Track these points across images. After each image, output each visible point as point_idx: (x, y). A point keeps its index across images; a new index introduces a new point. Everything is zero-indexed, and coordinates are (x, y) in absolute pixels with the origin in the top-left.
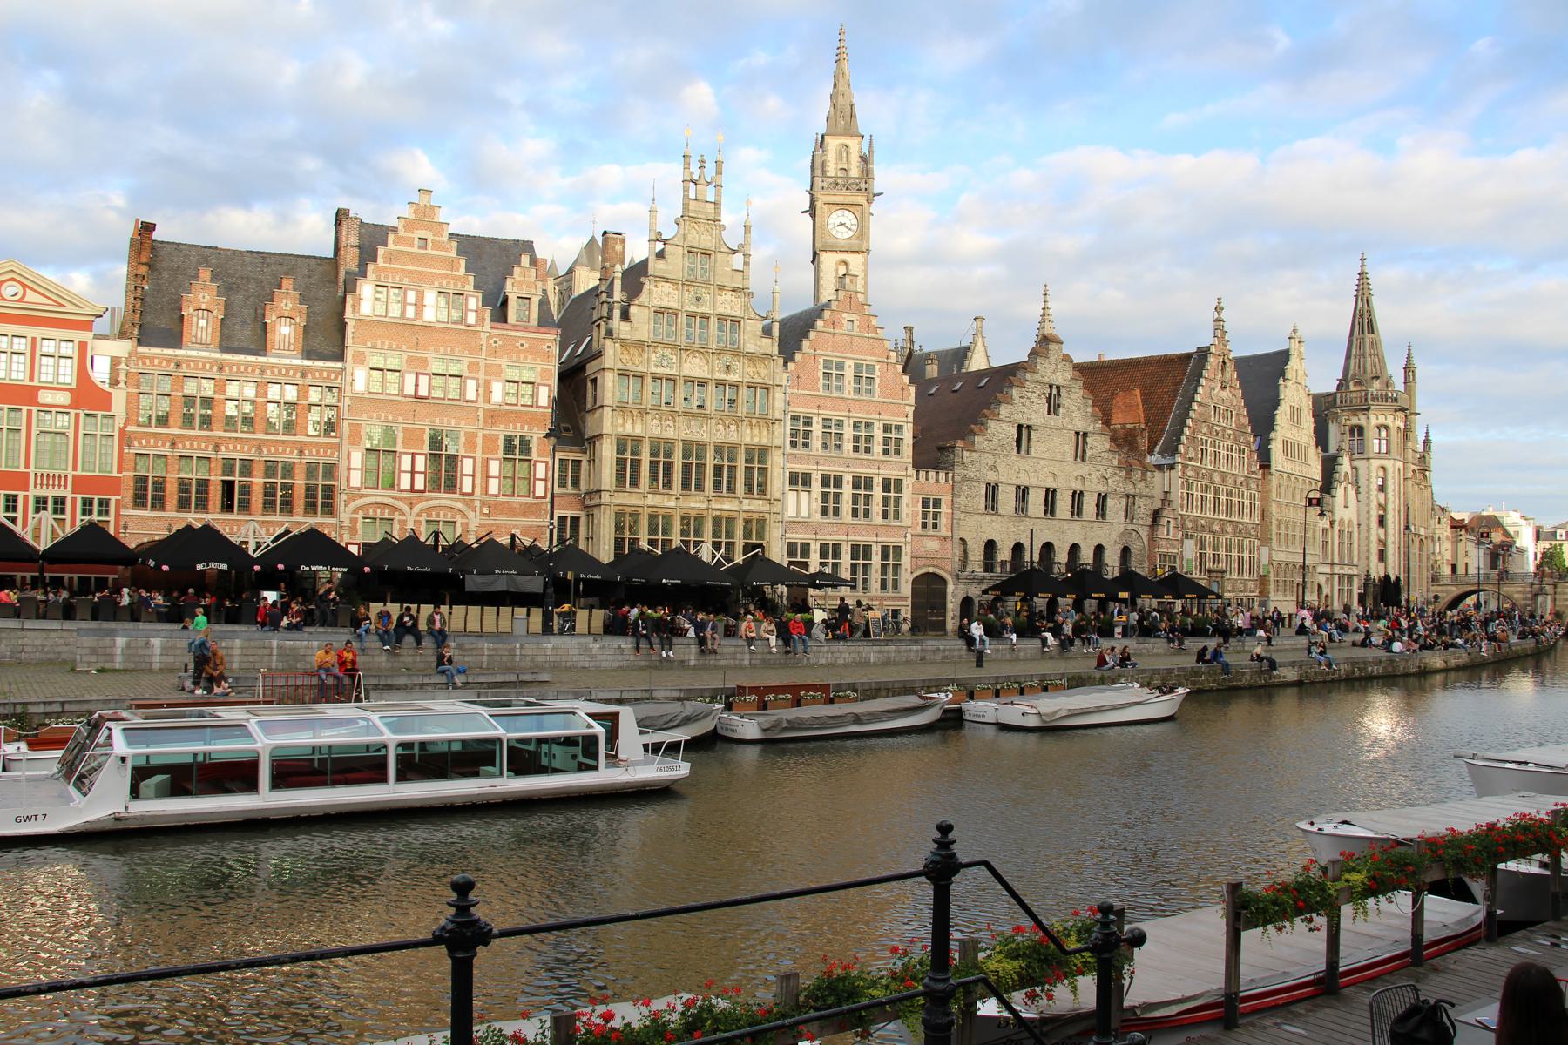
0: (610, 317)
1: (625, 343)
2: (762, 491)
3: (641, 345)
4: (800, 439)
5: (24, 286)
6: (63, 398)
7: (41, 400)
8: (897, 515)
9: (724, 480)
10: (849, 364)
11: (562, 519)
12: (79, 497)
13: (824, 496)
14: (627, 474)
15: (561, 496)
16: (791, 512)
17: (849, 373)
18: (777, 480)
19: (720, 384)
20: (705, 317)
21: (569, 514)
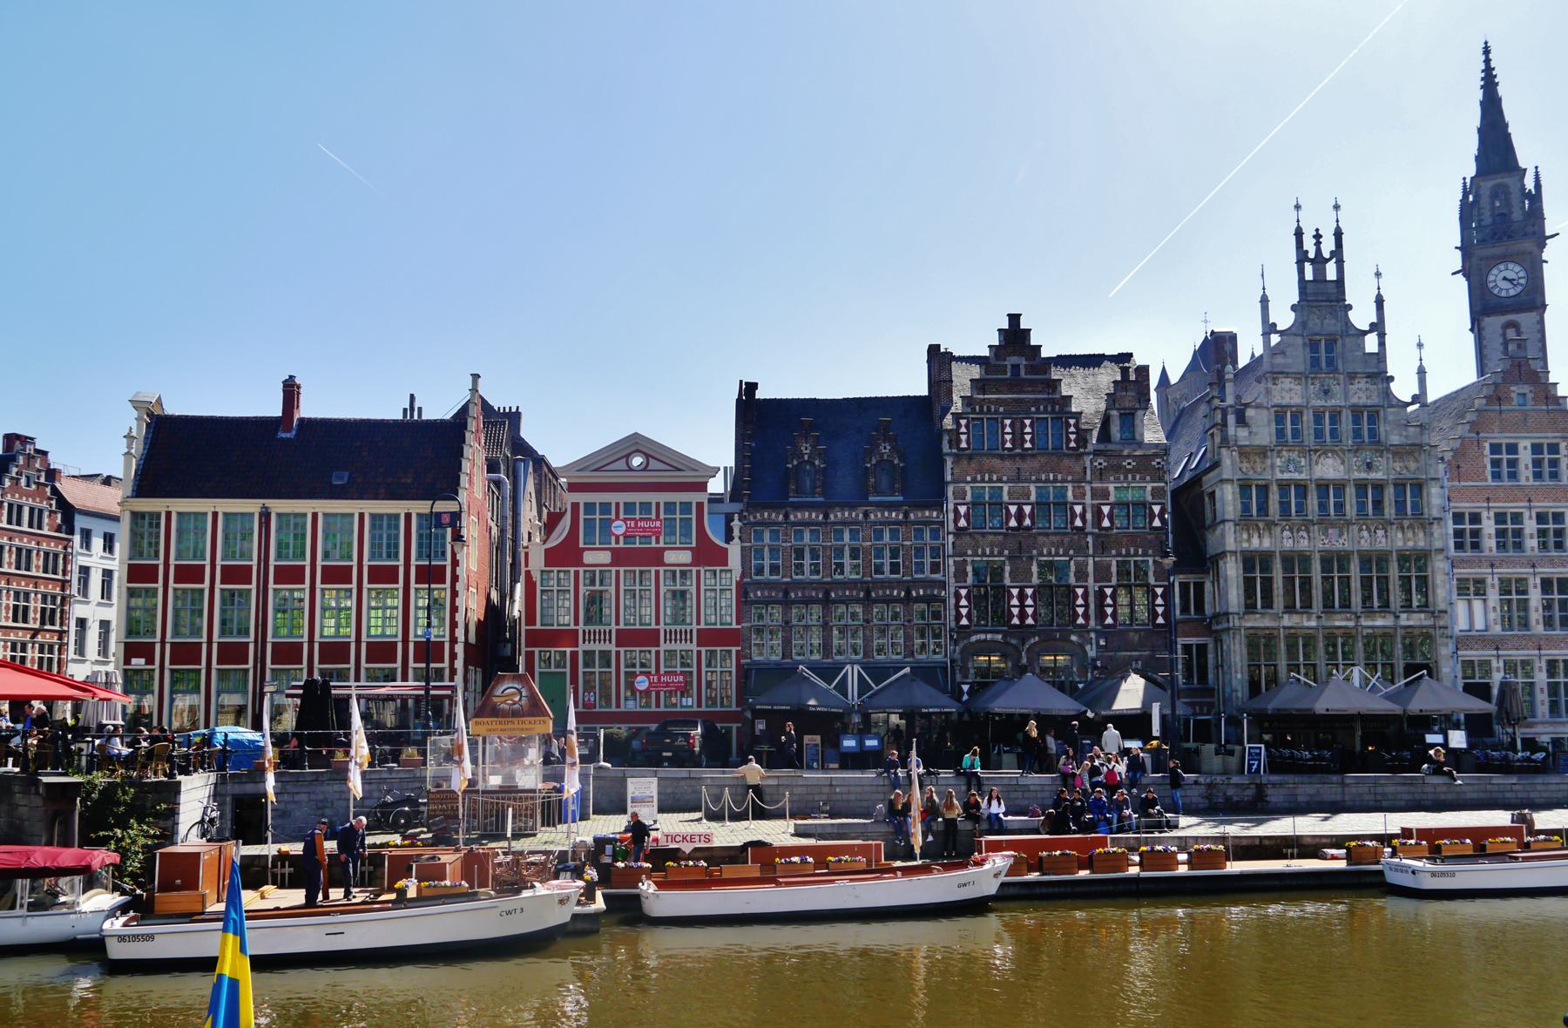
0: (1224, 424)
1: (1245, 453)
3: (1263, 452)
4: (1468, 540)
5: (647, 456)
6: (686, 557)
7: (667, 560)
9: (1376, 595)
10: (1525, 446)
11: (1187, 648)
12: (703, 649)
14: (1257, 593)
15: (1182, 622)
16: (1462, 624)
17: (1525, 457)
18: (1443, 589)
19: (1361, 487)
21: (1193, 640)
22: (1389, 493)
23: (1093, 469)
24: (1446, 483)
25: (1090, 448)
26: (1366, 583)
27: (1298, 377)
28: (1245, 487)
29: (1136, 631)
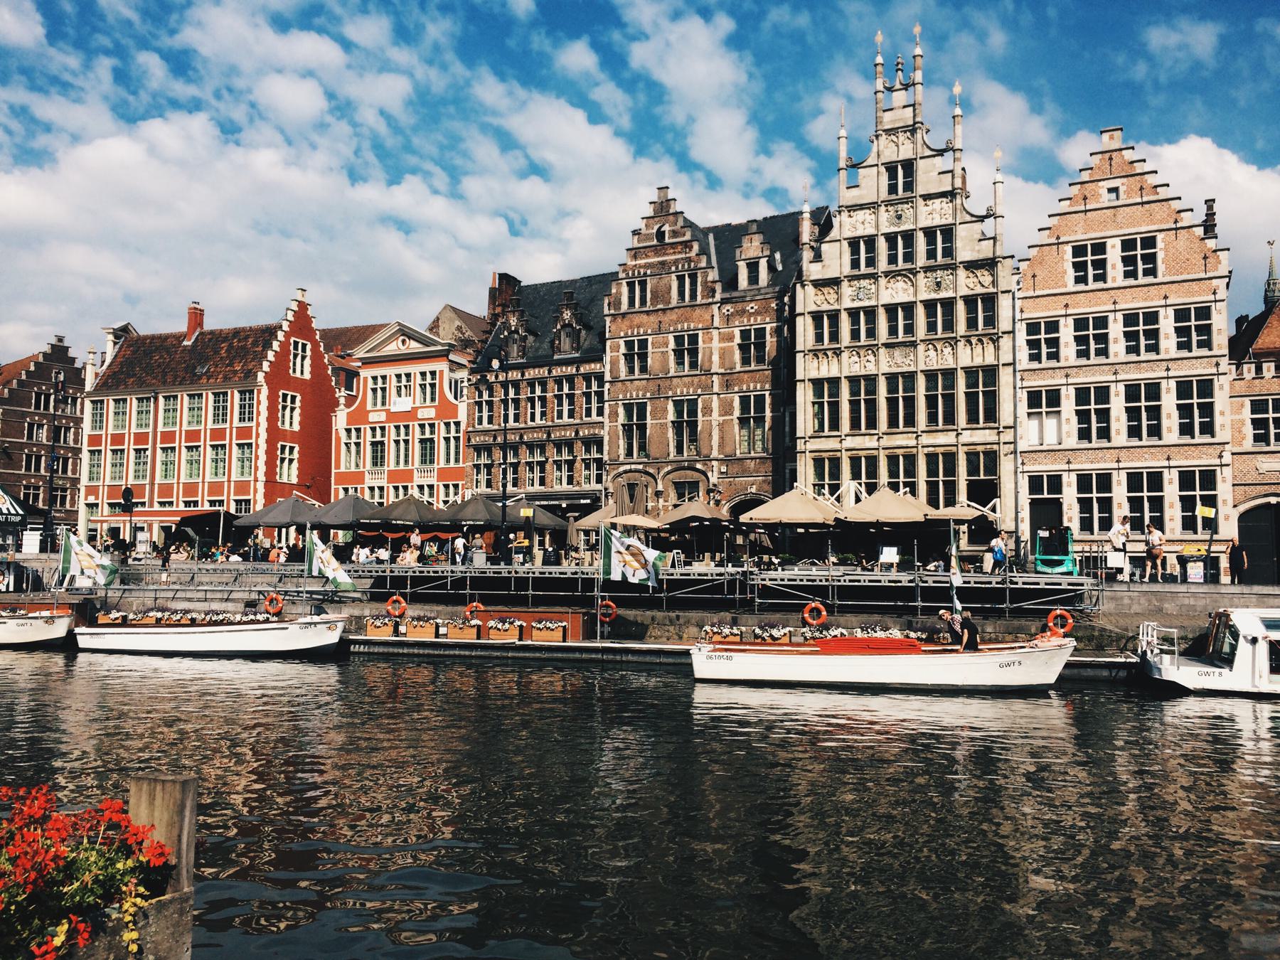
1: (819, 284)
2: (992, 415)
3: (835, 282)
6: (431, 413)
8: (1208, 429)
13: (1083, 416)
14: (829, 419)
19: (930, 306)
20: (909, 237)
22: (961, 308)
23: (722, 315)
24: (1018, 295)
25: (718, 297)
26: (931, 402)
27: (873, 206)
28: (817, 317)
29: (752, 459)
